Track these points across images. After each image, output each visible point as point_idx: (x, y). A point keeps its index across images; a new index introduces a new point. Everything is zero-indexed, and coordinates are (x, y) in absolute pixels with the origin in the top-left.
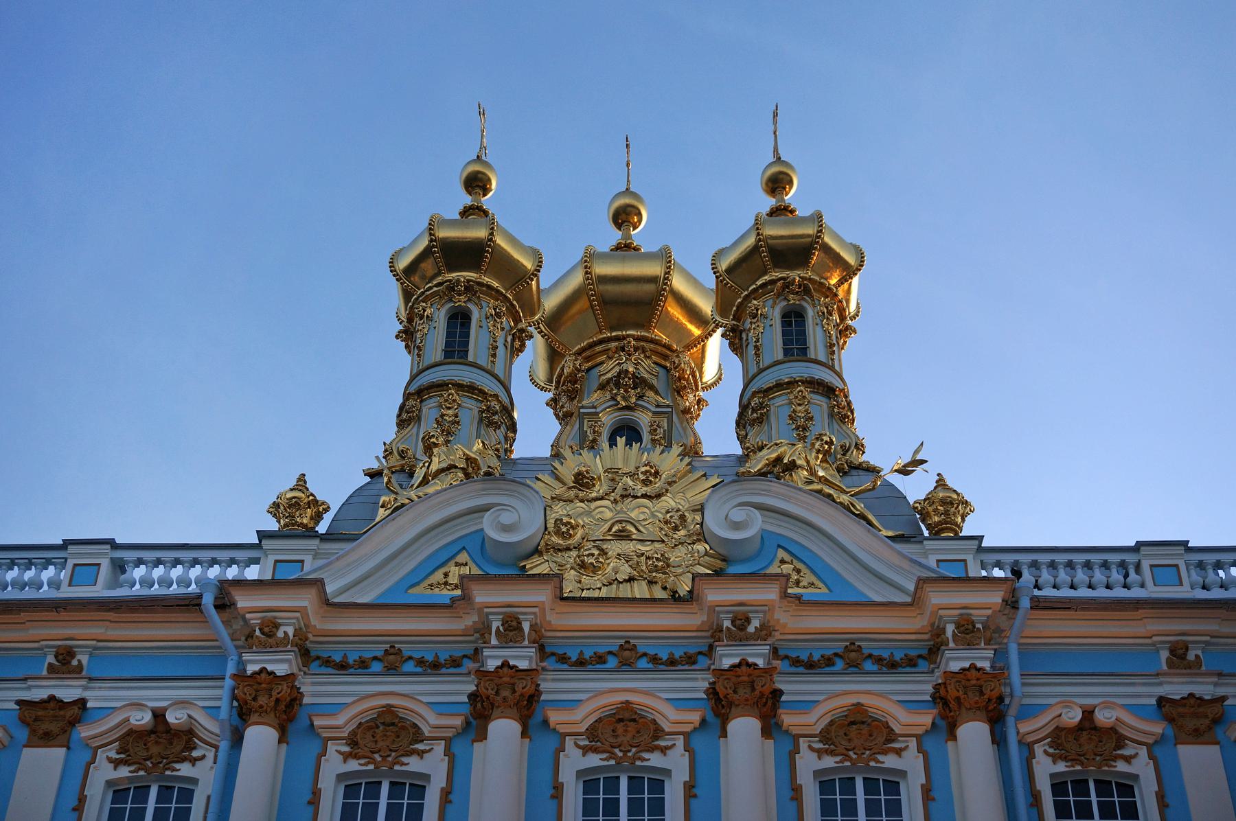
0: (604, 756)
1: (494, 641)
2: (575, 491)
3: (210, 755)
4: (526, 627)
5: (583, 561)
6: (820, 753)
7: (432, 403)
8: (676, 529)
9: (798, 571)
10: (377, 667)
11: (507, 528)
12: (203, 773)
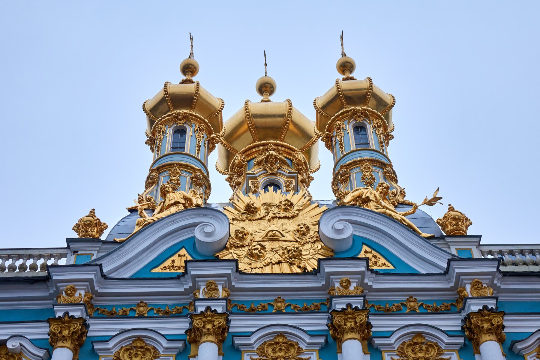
2: (246, 215)
5: (252, 253)
8: (304, 234)
9: (375, 257)
11: (209, 235)
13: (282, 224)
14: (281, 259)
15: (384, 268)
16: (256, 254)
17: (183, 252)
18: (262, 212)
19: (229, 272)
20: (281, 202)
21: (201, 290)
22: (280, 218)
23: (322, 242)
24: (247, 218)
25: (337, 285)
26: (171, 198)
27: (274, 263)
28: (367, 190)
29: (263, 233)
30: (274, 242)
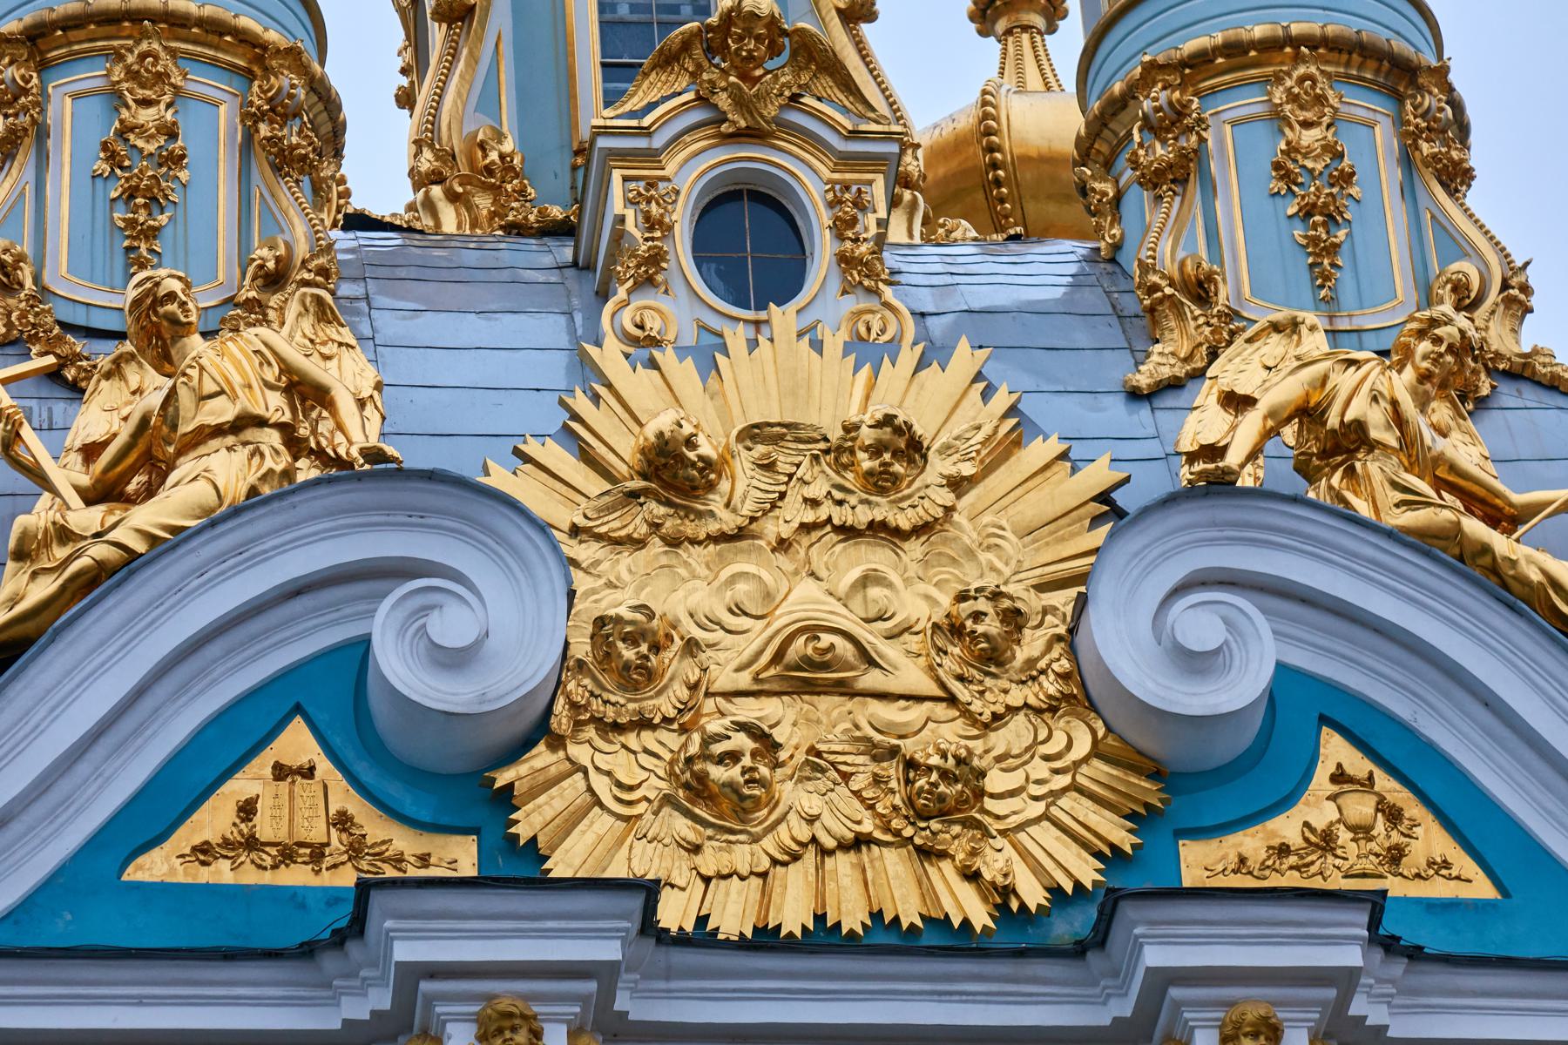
5: (702, 778)
7: (89, 76)
8: (992, 657)
9: (1393, 815)
13: (866, 581)
14: (868, 826)
15: (1440, 889)
16: (731, 785)
17: (297, 743)
18: (743, 484)
19: (609, 951)
20: (850, 429)
23: (1093, 707)
24: (655, 527)
26: (209, 387)
27: (830, 843)
29: (755, 637)
30: (825, 702)
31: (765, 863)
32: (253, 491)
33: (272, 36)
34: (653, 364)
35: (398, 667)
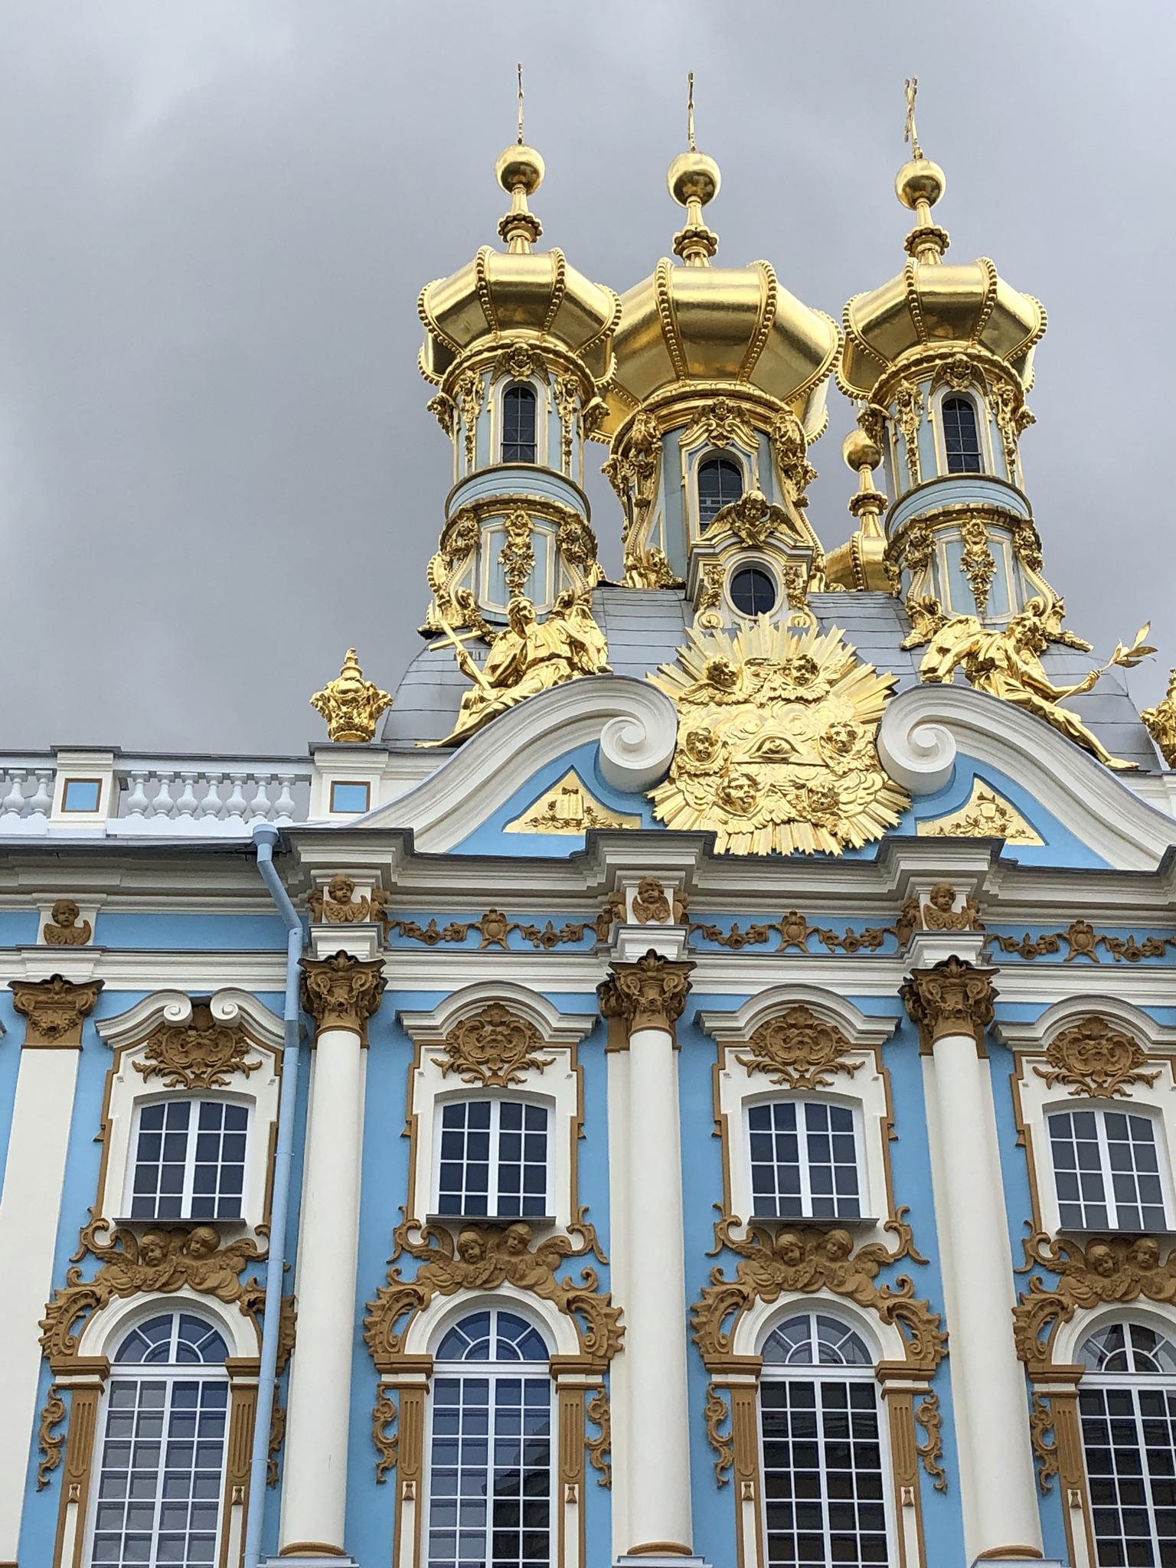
0: (776, 1077)
1: (632, 920)
2: (710, 689)
3: (269, 1063)
4: (669, 894)
5: (728, 795)
6: (1050, 1080)
7: (496, 525)
8: (844, 749)
9: (1003, 813)
10: (474, 940)
11: (630, 749)
12: (259, 1088)
14: (794, 814)
17: (571, 780)
21: (629, 900)
22: (788, 701)
23: (883, 769)
25: (924, 900)
27: (778, 821)
28: (990, 640)
29: (753, 742)
31: (752, 829)
32: (555, 683)
33: (568, 509)
34: (712, 635)
35: (611, 752)
